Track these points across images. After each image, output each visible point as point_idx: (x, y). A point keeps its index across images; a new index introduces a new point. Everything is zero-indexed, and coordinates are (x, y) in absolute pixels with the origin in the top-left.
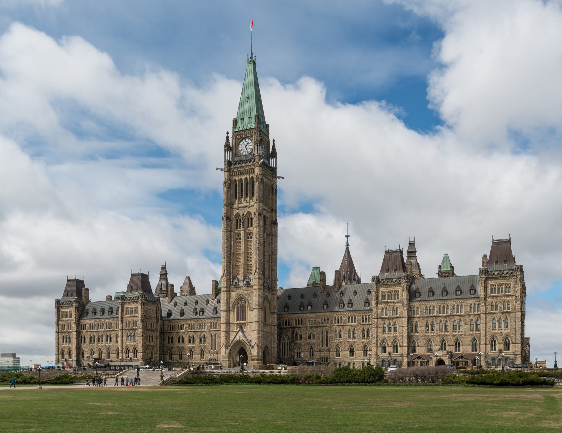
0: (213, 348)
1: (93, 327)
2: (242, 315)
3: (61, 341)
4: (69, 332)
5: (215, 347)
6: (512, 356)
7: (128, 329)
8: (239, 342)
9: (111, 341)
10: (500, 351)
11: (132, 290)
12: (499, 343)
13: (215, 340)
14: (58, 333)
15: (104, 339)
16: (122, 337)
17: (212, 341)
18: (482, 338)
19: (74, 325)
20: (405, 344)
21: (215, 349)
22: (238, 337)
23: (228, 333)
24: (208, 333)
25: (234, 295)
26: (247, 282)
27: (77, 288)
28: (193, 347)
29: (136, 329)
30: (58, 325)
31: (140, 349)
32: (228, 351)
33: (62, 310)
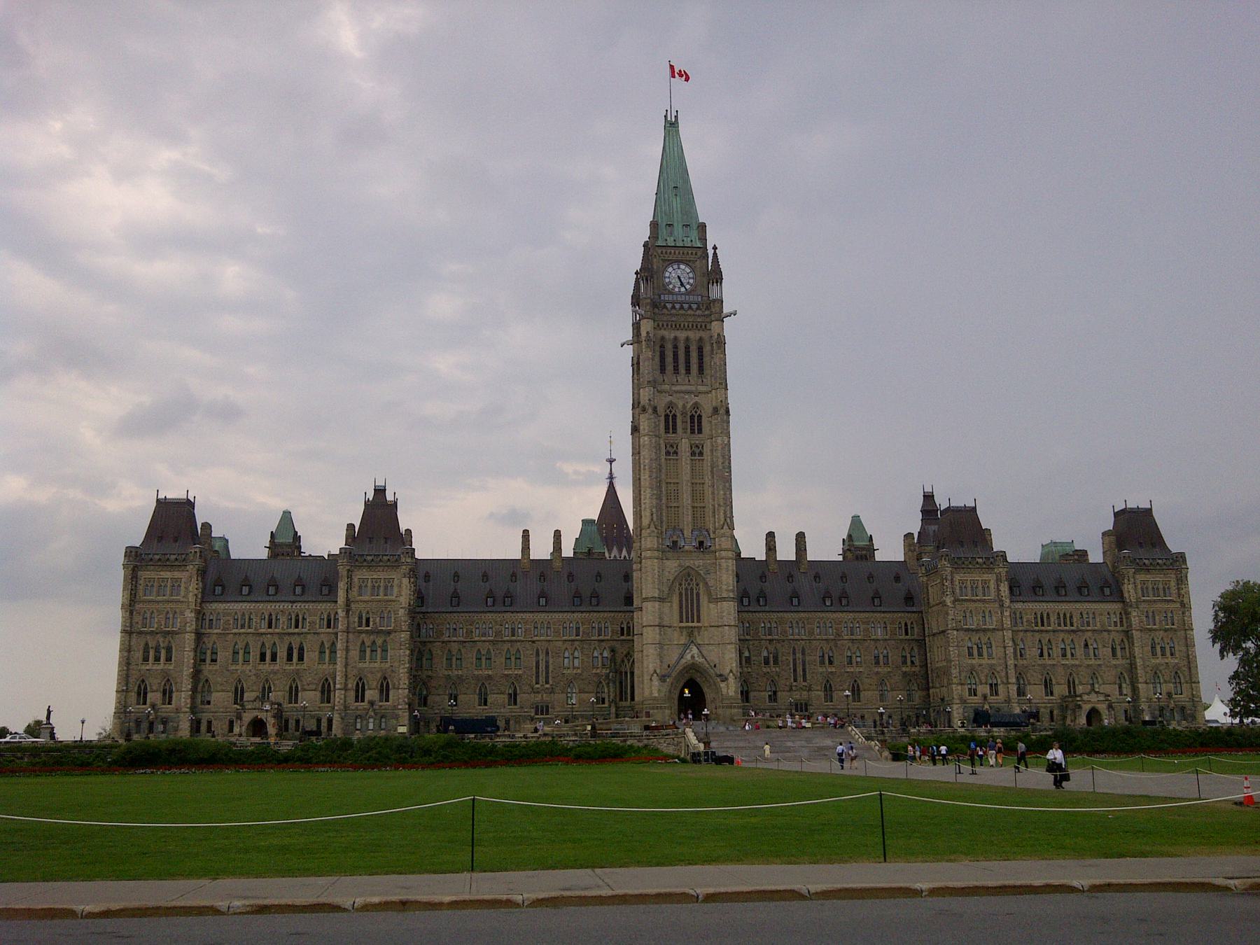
0: (542, 679)
1: (245, 621)
2: (690, 611)
3: (138, 655)
4: (168, 633)
5: (547, 677)
6: (1189, 705)
7: (367, 632)
8: (693, 667)
9: (301, 658)
10: (1169, 695)
11: (371, 539)
12: (1165, 682)
13: (547, 662)
14: (128, 632)
15: (282, 653)
16: (347, 650)
17: (538, 663)
18: (1140, 671)
19: (190, 615)
20: (1014, 680)
21: (547, 682)
22: (688, 657)
23: (661, 645)
24: (528, 645)
25: (672, 566)
26: (701, 543)
27: (174, 523)
28: (489, 676)
29: (389, 633)
30: (131, 613)
31: (402, 678)
32: (665, 688)
33: (143, 575)
